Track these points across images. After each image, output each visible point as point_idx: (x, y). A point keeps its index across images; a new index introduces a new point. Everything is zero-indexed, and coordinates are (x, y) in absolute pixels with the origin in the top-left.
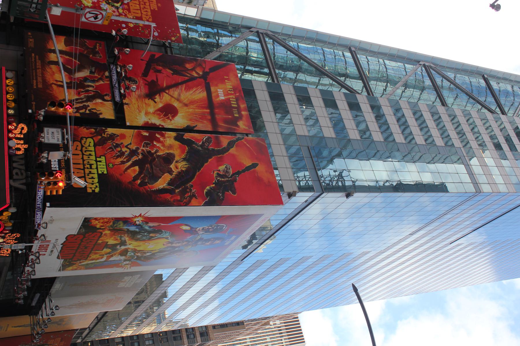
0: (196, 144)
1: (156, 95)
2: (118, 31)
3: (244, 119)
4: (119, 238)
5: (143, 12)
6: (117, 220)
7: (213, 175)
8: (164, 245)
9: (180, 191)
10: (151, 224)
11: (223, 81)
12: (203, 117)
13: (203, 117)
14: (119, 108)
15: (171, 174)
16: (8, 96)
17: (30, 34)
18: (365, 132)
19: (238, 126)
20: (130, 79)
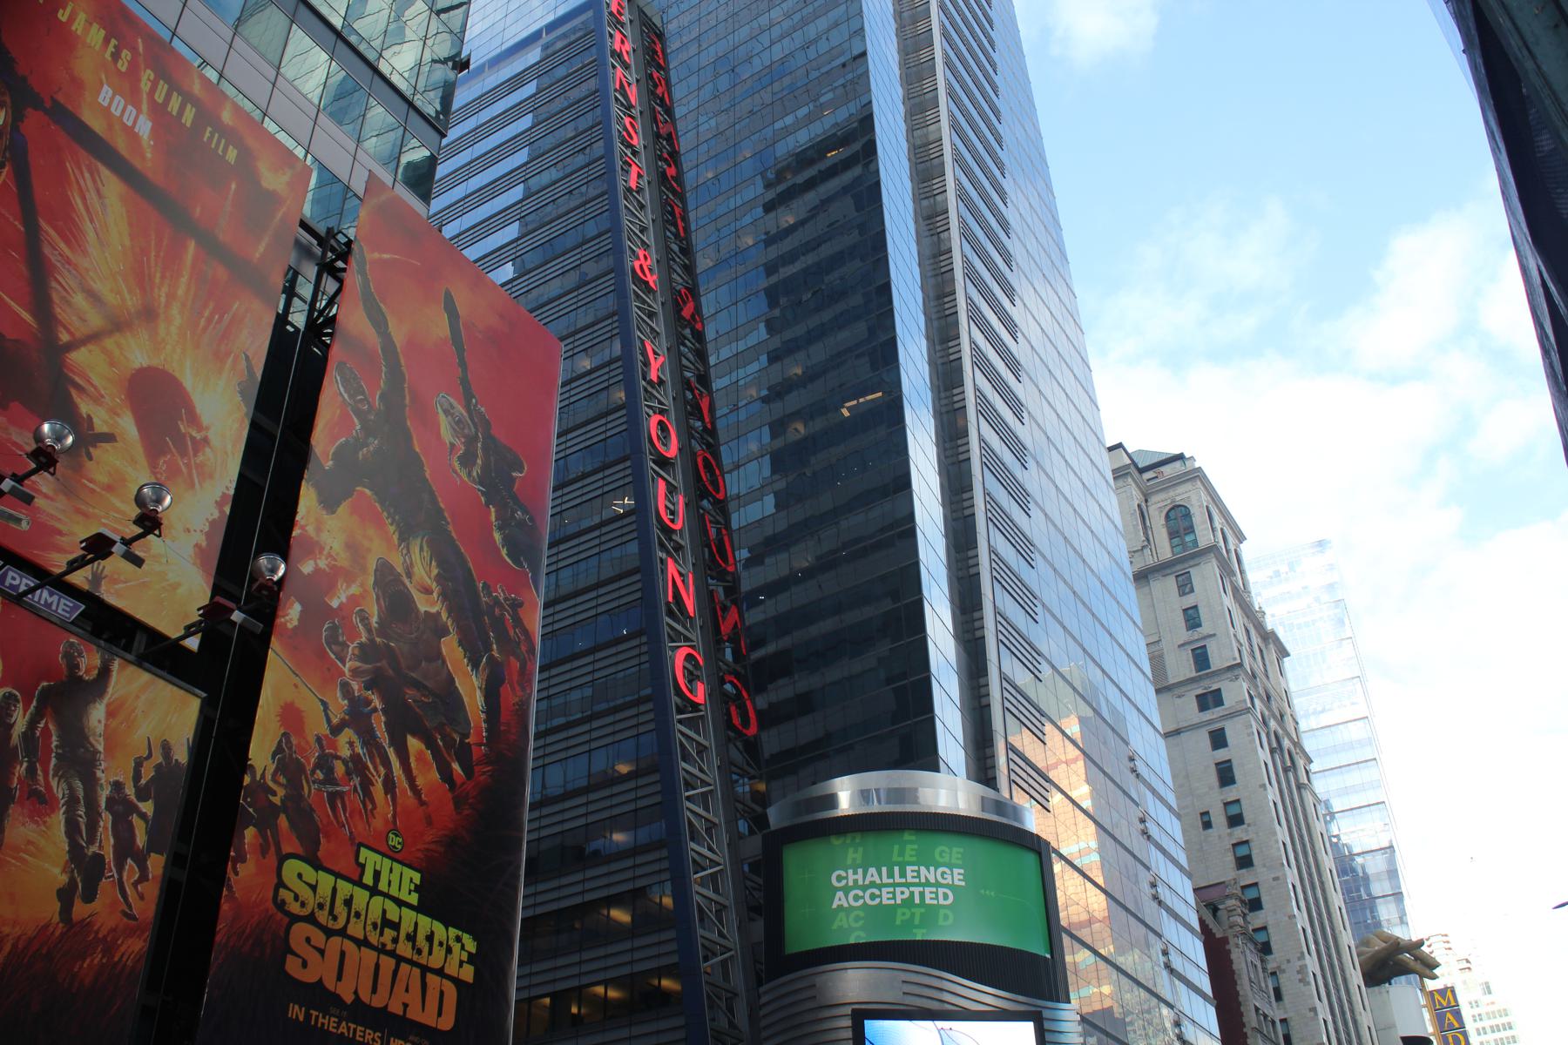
7: (462, 480)
15: (444, 632)
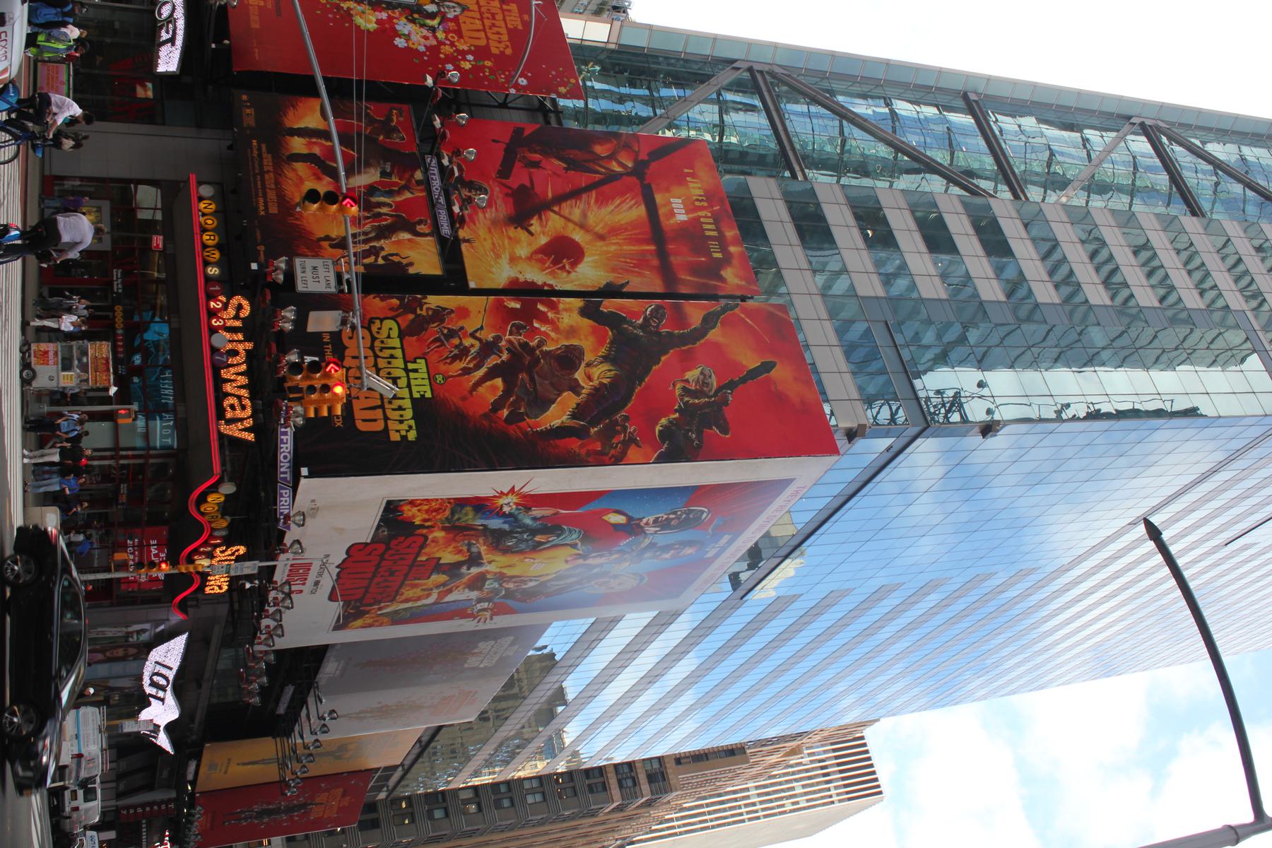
0: (631, 324)
1: (531, 217)
2: (440, 75)
3: (735, 262)
4: (465, 548)
5: (490, 36)
6: (461, 503)
8: (567, 562)
9: (601, 430)
10: (537, 512)
11: (681, 180)
12: (641, 263)
13: (641, 263)
14: (451, 251)
15: (578, 394)
16: (205, 237)
17: (245, 97)
18: (1016, 286)
19: (723, 280)
20: (470, 186)
